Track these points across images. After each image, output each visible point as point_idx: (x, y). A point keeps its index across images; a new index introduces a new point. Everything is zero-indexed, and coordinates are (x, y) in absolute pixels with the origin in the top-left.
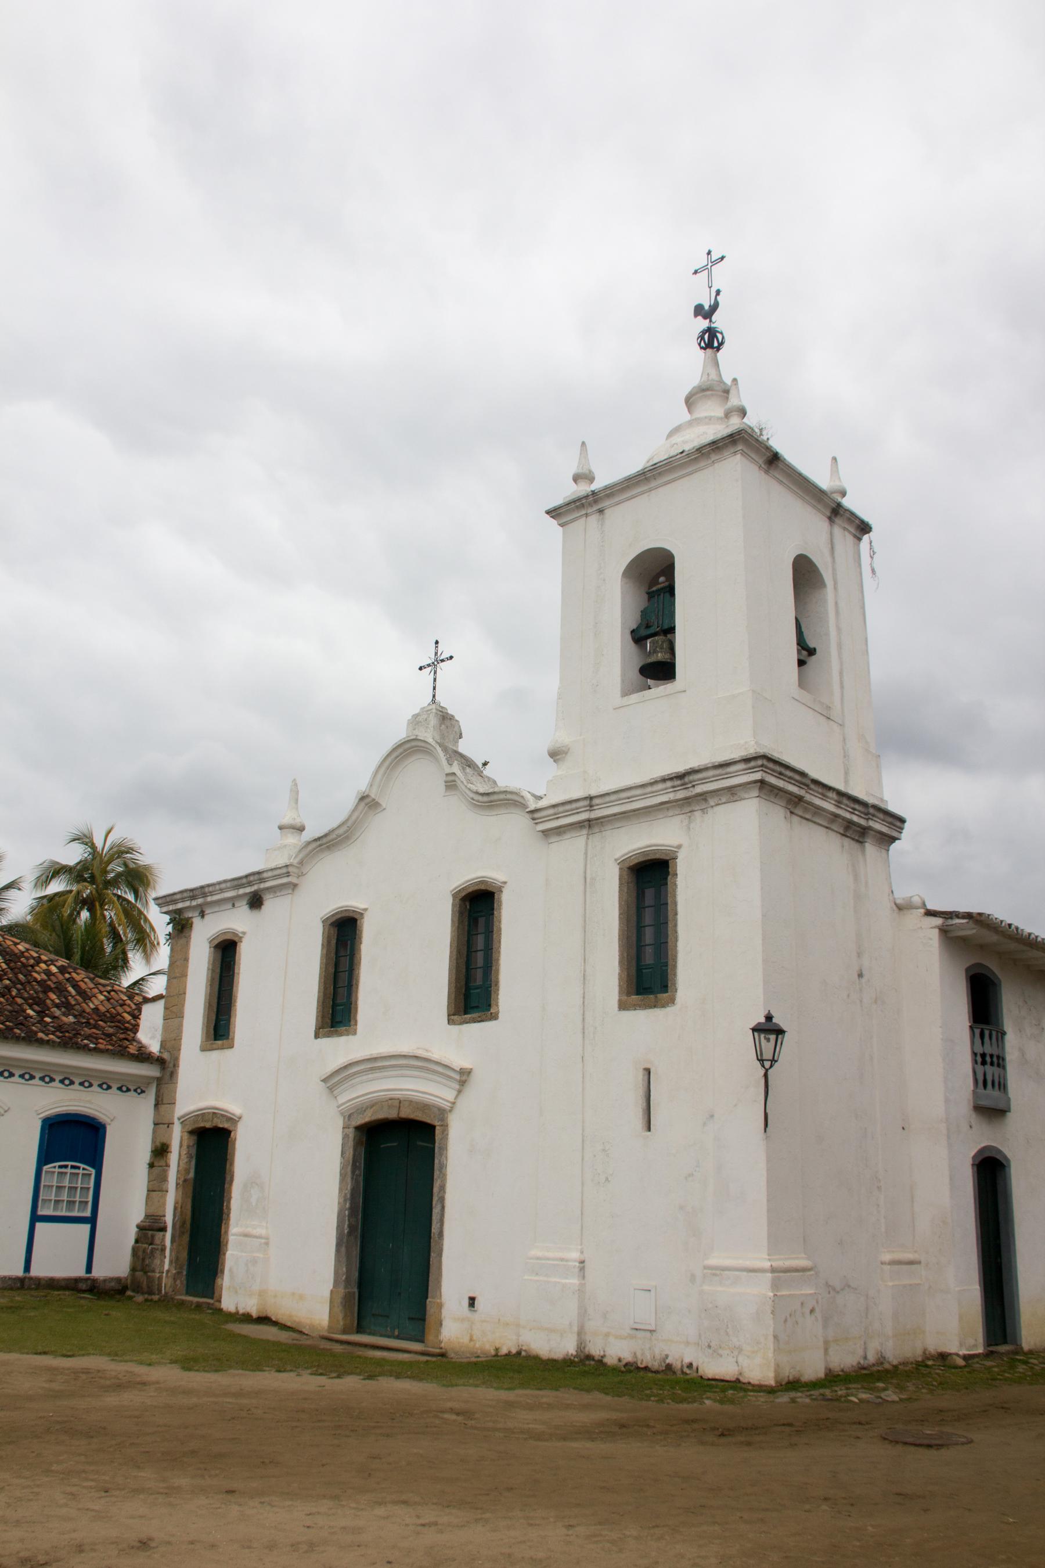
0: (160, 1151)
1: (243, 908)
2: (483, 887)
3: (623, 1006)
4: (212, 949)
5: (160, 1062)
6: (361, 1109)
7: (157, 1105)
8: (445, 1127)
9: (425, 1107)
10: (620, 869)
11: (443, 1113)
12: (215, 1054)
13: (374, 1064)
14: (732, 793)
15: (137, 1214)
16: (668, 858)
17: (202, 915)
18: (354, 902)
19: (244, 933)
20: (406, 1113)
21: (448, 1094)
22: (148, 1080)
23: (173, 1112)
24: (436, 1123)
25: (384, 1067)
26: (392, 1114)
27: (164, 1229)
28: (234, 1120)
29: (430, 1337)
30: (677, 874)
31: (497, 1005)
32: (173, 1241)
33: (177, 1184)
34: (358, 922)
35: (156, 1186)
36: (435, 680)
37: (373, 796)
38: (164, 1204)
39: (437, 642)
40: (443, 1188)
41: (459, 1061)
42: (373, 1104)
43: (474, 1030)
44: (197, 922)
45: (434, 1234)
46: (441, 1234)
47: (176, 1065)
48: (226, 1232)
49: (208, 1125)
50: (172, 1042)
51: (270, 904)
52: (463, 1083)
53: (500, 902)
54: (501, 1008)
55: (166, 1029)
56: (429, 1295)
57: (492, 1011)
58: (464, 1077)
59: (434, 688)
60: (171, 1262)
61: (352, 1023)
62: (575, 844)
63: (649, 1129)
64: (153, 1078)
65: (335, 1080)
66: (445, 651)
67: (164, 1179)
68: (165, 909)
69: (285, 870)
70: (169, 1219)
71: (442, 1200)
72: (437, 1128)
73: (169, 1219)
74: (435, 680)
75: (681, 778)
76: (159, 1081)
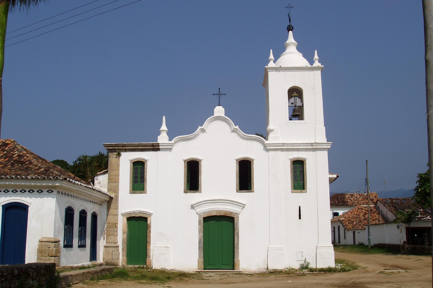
2: (247, 159)
3: (292, 192)
4: (132, 163)
6: (204, 213)
8: (238, 217)
9: (231, 213)
10: (290, 161)
12: (138, 196)
13: (214, 201)
16: (304, 160)
19: (148, 160)
21: (240, 210)
23: (118, 212)
24: (235, 217)
25: (216, 202)
27: (118, 247)
28: (150, 215)
29: (236, 267)
30: (306, 164)
31: (254, 189)
32: (123, 249)
33: (124, 233)
34: (199, 163)
36: (219, 99)
37: (204, 128)
38: (117, 239)
39: (219, 89)
40: (238, 232)
42: (210, 212)
45: (236, 243)
46: (238, 243)
48: (149, 246)
49: (138, 216)
52: (244, 207)
53: (253, 164)
54: (254, 190)
56: (235, 258)
57: (252, 190)
59: (219, 101)
60: (123, 256)
61: (199, 189)
63: (300, 218)
64: (106, 201)
66: (222, 92)
68: (106, 148)
71: (238, 235)
72: (235, 218)
74: (219, 99)
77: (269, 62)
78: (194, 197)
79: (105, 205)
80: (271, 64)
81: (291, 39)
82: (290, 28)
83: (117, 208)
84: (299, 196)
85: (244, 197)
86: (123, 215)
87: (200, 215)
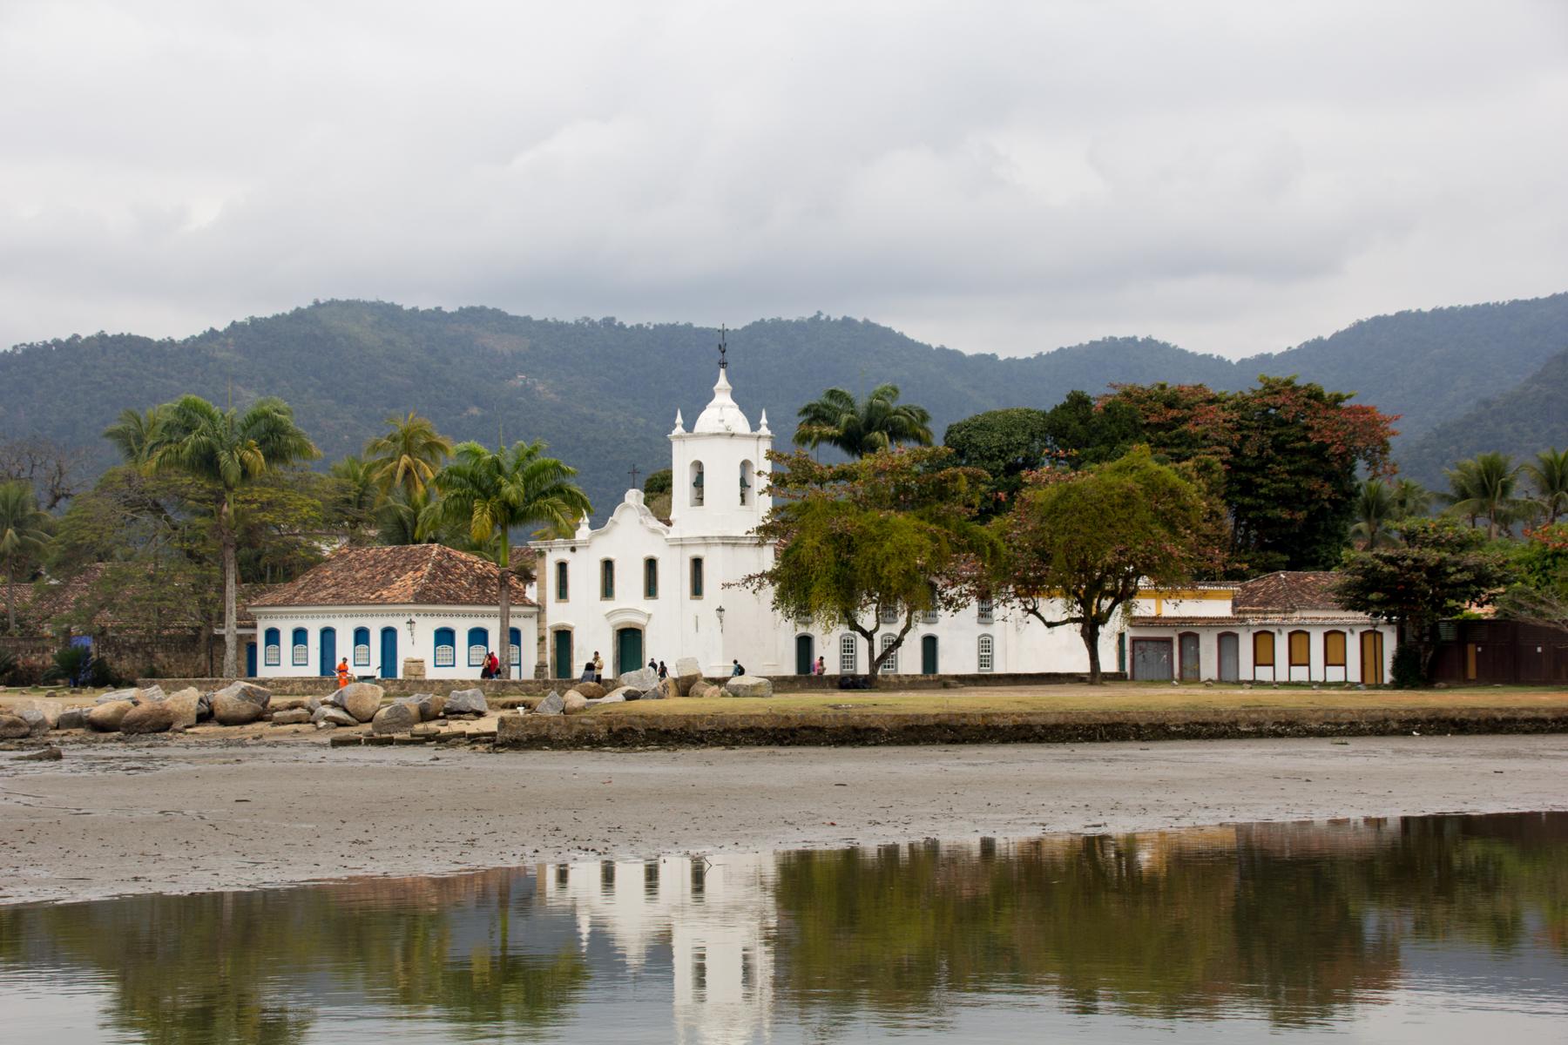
0: (542, 639)
1: (568, 551)
5: (539, 606)
6: (619, 625)
7: (538, 622)
9: (638, 624)
11: (644, 626)
12: (562, 605)
13: (622, 611)
14: (716, 544)
15: (534, 662)
17: (550, 551)
18: (611, 556)
20: (633, 626)
22: (533, 613)
26: (628, 626)
28: (572, 628)
35: (541, 650)
41: (649, 612)
42: (622, 623)
43: (651, 602)
44: (548, 553)
47: (545, 607)
50: (542, 599)
51: (578, 551)
55: (539, 594)
58: (649, 616)
62: (678, 549)
65: (609, 615)
67: (544, 648)
69: (585, 542)
70: (549, 663)
73: (549, 663)
75: (704, 538)
76: (538, 613)
77: (675, 426)
78: (609, 605)
79: (536, 616)
80: (679, 430)
81: (723, 381)
82: (723, 364)
83: (545, 621)
84: (696, 603)
85: (648, 606)
86: (551, 628)
87: (614, 627)
